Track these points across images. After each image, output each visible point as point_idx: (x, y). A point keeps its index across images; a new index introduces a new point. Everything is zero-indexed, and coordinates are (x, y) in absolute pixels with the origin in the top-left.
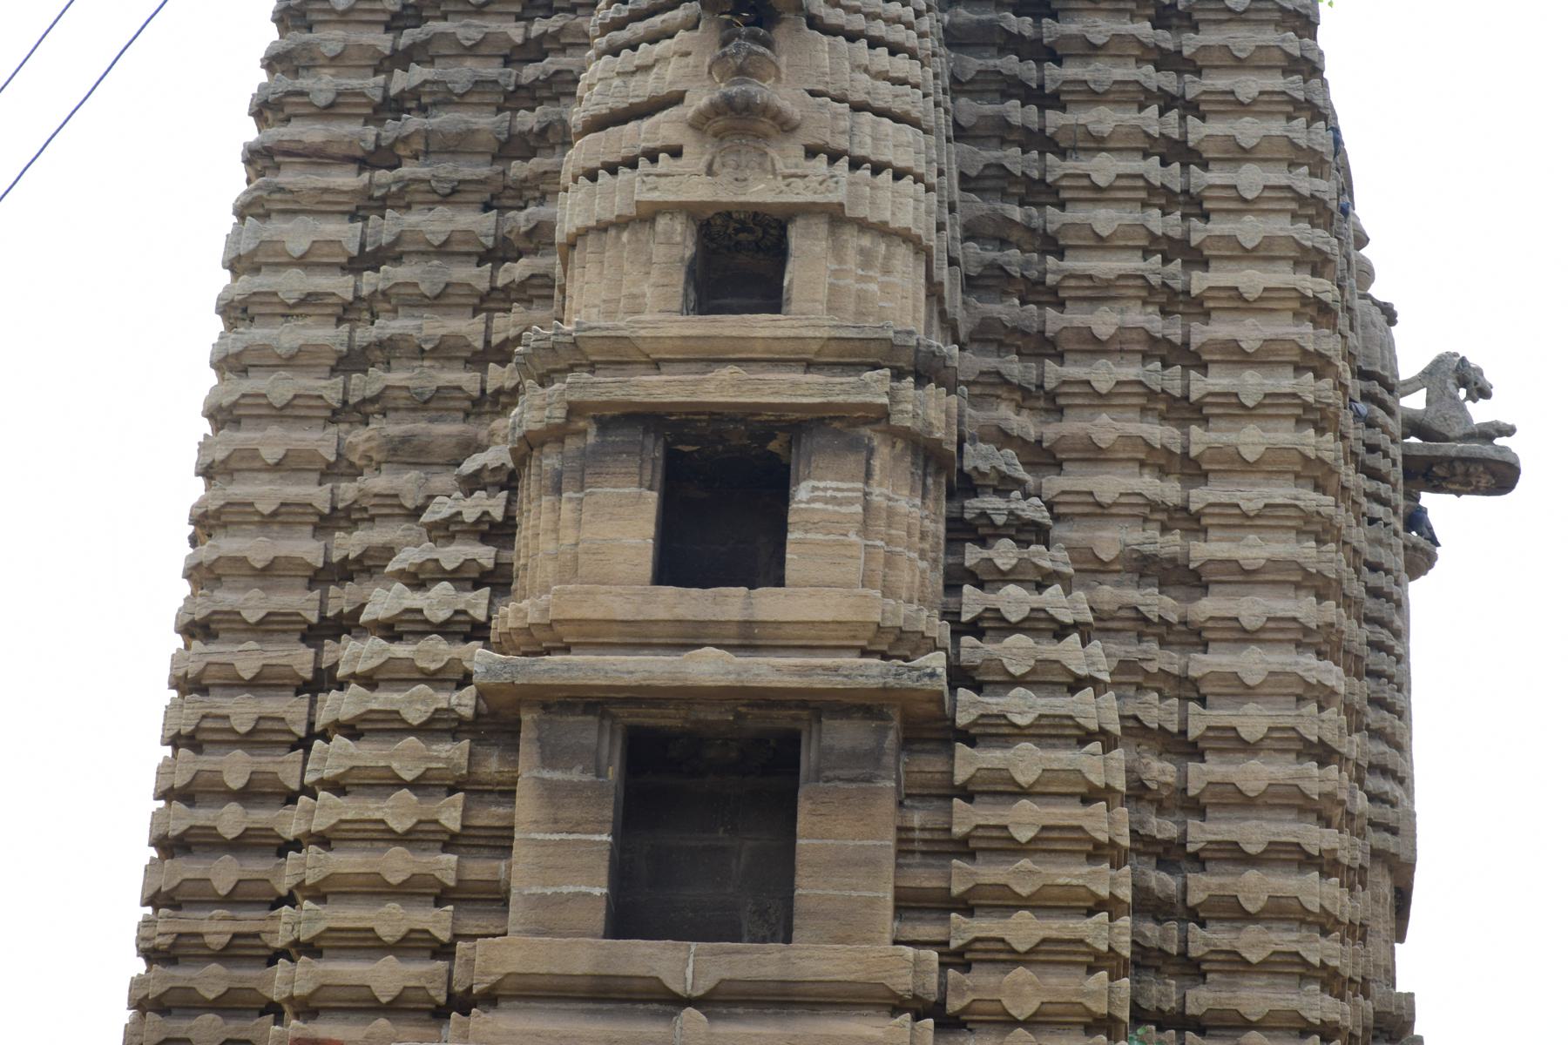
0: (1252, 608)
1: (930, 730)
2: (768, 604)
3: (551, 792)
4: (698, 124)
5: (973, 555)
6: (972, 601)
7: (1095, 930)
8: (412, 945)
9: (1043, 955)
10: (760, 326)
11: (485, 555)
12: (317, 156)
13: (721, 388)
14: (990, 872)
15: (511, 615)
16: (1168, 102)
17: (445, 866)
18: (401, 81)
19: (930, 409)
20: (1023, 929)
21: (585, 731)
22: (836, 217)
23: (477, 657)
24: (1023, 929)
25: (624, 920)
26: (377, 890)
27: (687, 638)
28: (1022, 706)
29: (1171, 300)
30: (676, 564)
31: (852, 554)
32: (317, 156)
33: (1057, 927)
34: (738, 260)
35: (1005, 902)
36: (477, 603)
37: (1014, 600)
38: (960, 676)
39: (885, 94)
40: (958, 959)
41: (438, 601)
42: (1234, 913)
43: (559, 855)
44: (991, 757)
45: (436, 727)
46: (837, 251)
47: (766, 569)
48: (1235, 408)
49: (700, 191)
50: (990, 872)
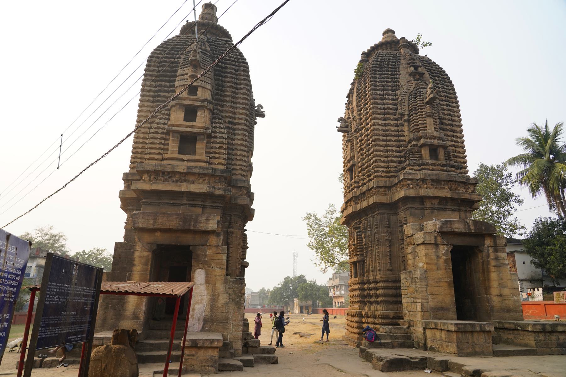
0: (240, 127)
1: (209, 136)
2: (194, 124)
3: (173, 140)
4: (189, 77)
5: (214, 121)
7: (223, 156)
8: (159, 154)
9: (219, 158)
10: (195, 97)
11: (167, 117)
12: (151, 75)
13: (190, 103)
14: (214, 150)
15: (169, 123)
16: (235, 78)
17: (162, 146)
18: (160, 69)
19: (211, 106)
20: (217, 156)
21: (176, 135)
22: (202, 87)
23: (166, 127)
24: (217, 156)
25: (179, 153)
26: (156, 148)
27: (187, 126)
28: (218, 135)
29: (234, 97)
31: (202, 119)
32: (151, 75)
33: (220, 156)
34: (193, 90)
35: (215, 153)
36: (166, 122)
37: (218, 125)
38: (212, 132)
40: (211, 158)
41: (162, 121)
43: (173, 146)
44: (215, 139)
45: (162, 133)
46: (202, 90)
47: (194, 121)
48: (239, 108)
50: (214, 150)
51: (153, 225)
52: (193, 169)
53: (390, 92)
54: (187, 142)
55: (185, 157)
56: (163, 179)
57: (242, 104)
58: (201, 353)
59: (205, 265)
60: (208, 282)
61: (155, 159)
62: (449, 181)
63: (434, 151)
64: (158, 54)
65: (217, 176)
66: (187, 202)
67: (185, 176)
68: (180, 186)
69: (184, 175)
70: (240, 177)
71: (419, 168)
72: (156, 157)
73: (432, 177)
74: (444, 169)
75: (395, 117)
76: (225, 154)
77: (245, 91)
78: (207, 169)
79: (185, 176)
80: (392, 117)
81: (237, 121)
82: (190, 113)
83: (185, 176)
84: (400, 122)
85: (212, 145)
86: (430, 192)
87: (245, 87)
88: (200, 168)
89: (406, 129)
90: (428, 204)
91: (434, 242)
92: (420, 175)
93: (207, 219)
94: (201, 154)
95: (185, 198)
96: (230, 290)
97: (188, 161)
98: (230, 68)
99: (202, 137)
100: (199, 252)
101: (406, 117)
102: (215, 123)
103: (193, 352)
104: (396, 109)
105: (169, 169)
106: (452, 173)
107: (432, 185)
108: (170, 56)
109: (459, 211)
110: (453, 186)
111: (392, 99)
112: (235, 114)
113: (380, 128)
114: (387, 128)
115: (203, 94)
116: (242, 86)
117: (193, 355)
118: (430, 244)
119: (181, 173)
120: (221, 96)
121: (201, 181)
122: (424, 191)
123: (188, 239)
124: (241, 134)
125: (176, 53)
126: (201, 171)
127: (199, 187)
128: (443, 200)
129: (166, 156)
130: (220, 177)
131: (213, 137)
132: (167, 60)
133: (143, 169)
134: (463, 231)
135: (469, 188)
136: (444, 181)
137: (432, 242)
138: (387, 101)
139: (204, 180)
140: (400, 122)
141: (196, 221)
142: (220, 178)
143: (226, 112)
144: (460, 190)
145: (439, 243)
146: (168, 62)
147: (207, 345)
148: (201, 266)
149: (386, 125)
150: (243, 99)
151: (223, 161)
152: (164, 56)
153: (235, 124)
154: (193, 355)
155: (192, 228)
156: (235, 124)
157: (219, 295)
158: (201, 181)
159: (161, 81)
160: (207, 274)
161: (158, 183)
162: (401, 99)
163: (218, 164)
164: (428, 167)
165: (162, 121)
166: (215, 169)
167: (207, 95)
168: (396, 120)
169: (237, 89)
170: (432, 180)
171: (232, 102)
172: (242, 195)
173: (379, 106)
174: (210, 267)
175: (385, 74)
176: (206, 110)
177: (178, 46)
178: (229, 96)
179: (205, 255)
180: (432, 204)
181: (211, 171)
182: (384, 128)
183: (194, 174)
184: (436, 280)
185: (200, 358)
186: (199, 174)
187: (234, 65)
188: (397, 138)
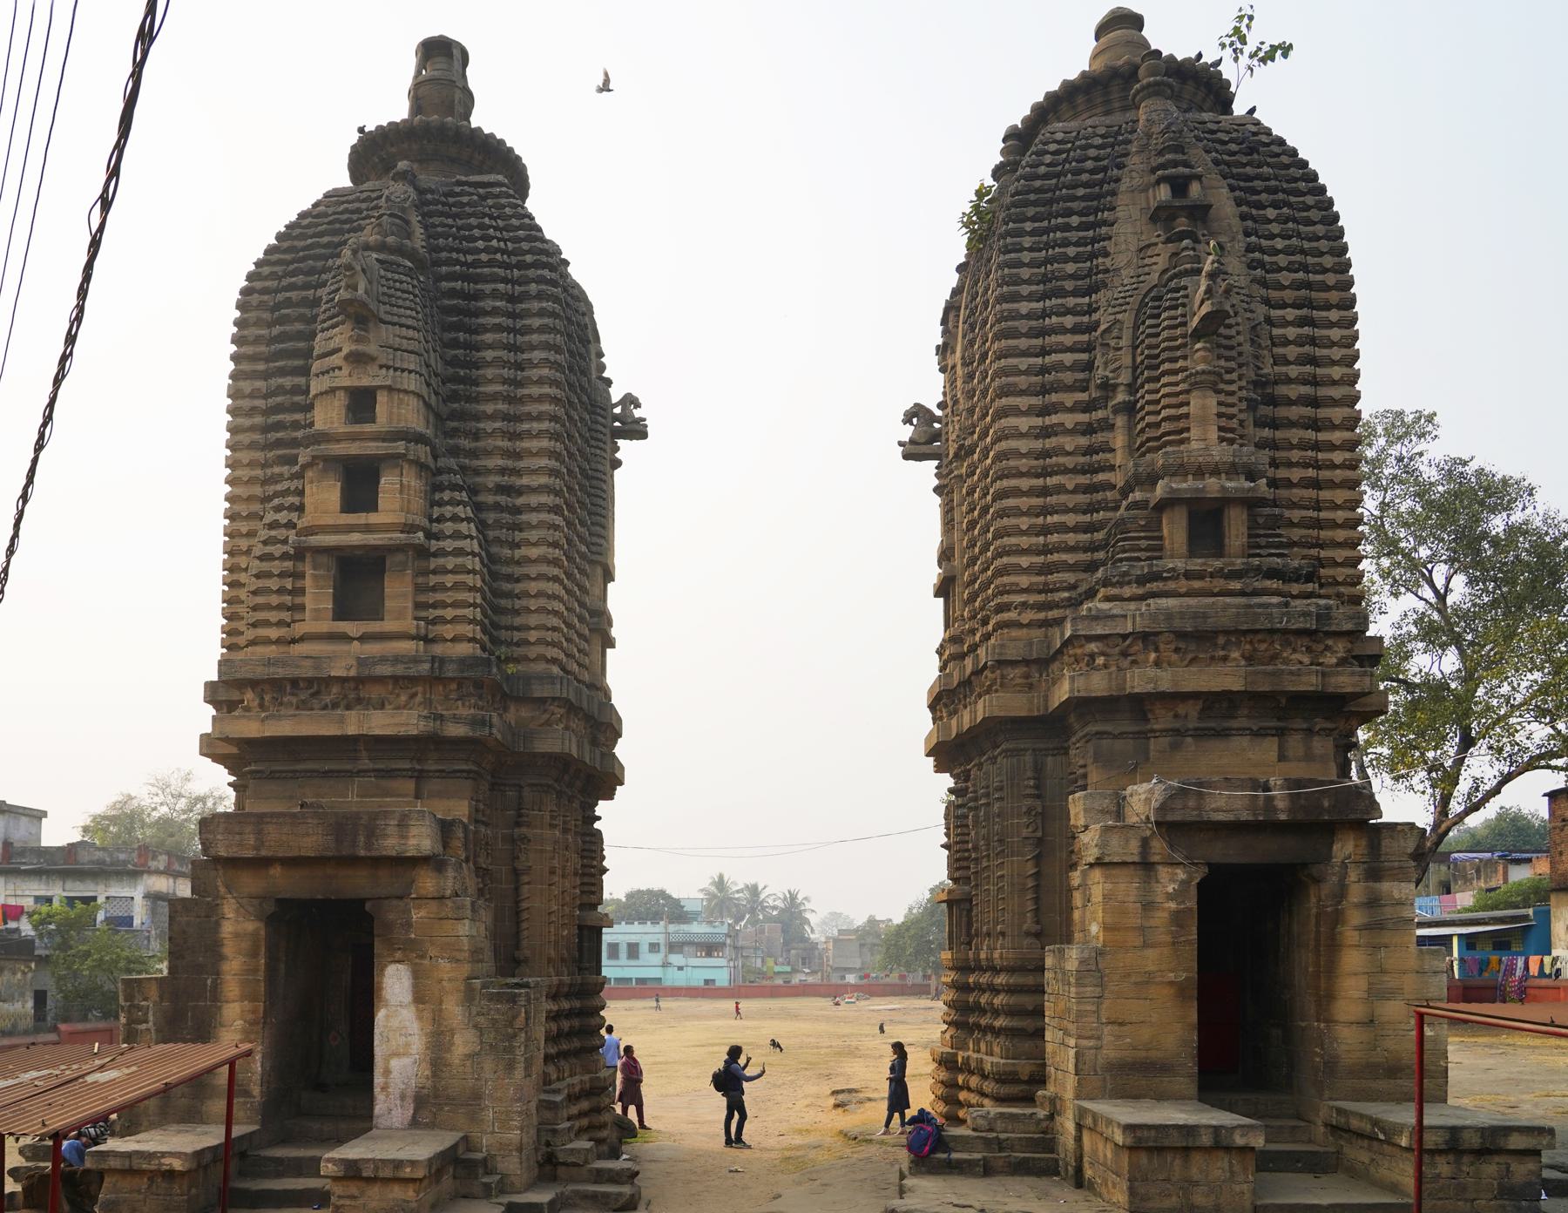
1: (422, 553)
2: (373, 518)
3: (315, 577)
6: (436, 512)
7: (468, 612)
8: (281, 623)
9: (455, 620)
14: (439, 596)
16: (509, 330)
17: (288, 599)
19: (423, 452)
20: (449, 613)
21: (323, 559)
23: (292, 536)
24: (449, 613)
26: (268, 607)
27: (350, 529)
28: (449, 545)
29: (510, 400)
30: (349, 505)
31: (397, 498)
33: (460, 612)
35: (444, 605)
36: (294, 516)
37: (448, 510)
40: (434, 621)
41: (283, 517)
42: (527, 594)
43: (318, 597)
44: (441, 561)
45: (285, 556)
48: (529, 435)
50: (439, 596)
52: (375, 664)
54: (357, 577)
55: (351, 628)
56: (294, 700)
57: (539, 418)
58: (375, 1191)
61: (267, 641)
64: (266, 278)
65: (452, 679)
66: (371, 766)
67: (357, 689)
68: (342, 721)
69: (352, 685)
70: (540, 667)
71: (1140, 591)
72: (273, 633)
75: (1084, 396)
76: (475, 605)
77: (545, 372)
78: (416, 660)
79: (356, 688)
80: (1069, 399)
81: (525, 481)
82: (359, 485)
83: (357, 689)
84: (1100, 414)
85: (433, 580)
86: (1165, 680)
87: (543, 355)
88: (397, 659)
89: (1119, 440)
90: (1162, 719)
93: (403, 824)
94: (400, 615)
95: (364, 754)
97: (363, 638)
98: (495, 295)
99: (400, 557)
101: (1121, 397)
102: (441, 504)
103: (353, 1189)
104: (1089, 366)
108: (300, 279)
109: (1281, 733)
111: (1076, 330)
112: (517, 455)
114: (1051, 443)
115: (401, 412)
116: (537, 355)
117: (353, 1197)
119: (342, 680)
120: (469, 399)
121: (403, 698)
122: (1140, 679)
124: (540, 525)
125: (320, 264)
126: (400, 670)
127: (397, 720)
129: (299, 629)
130: (460, 682)
131: (435, 555)
132: (293, 295)
133: (238, 676)
138: (1054, 339)
139: (413, 696)
140: (1100, 414)
141: (372, 833)
142: (460, 686)
143: (488, 453)
146: (298, 305)
149: (1046, 432)
150: (540, 399)
151: (467, 630)
152: (285, 282)
153: (519, 492)
154: (353, 1197)
155: (362, 853)
156: (519, 492)
158: (403, 698)
159: (282, 372)
161: (279, 718)
163: (453, 640)
165: (283, 517)
166: (442, 661)
167: (411, 416)
168: (1088, 407)
169: (519, 366)
171: (506, 417)
172: (548, 723)
173: (1023, 363)
176: (406, 466)
177: (325, 239)
180: (1176, 716)
181: (427, 666)
183: (380, 680)
185: (374, 1204)
186: (395, 679)
187: (505, 281)
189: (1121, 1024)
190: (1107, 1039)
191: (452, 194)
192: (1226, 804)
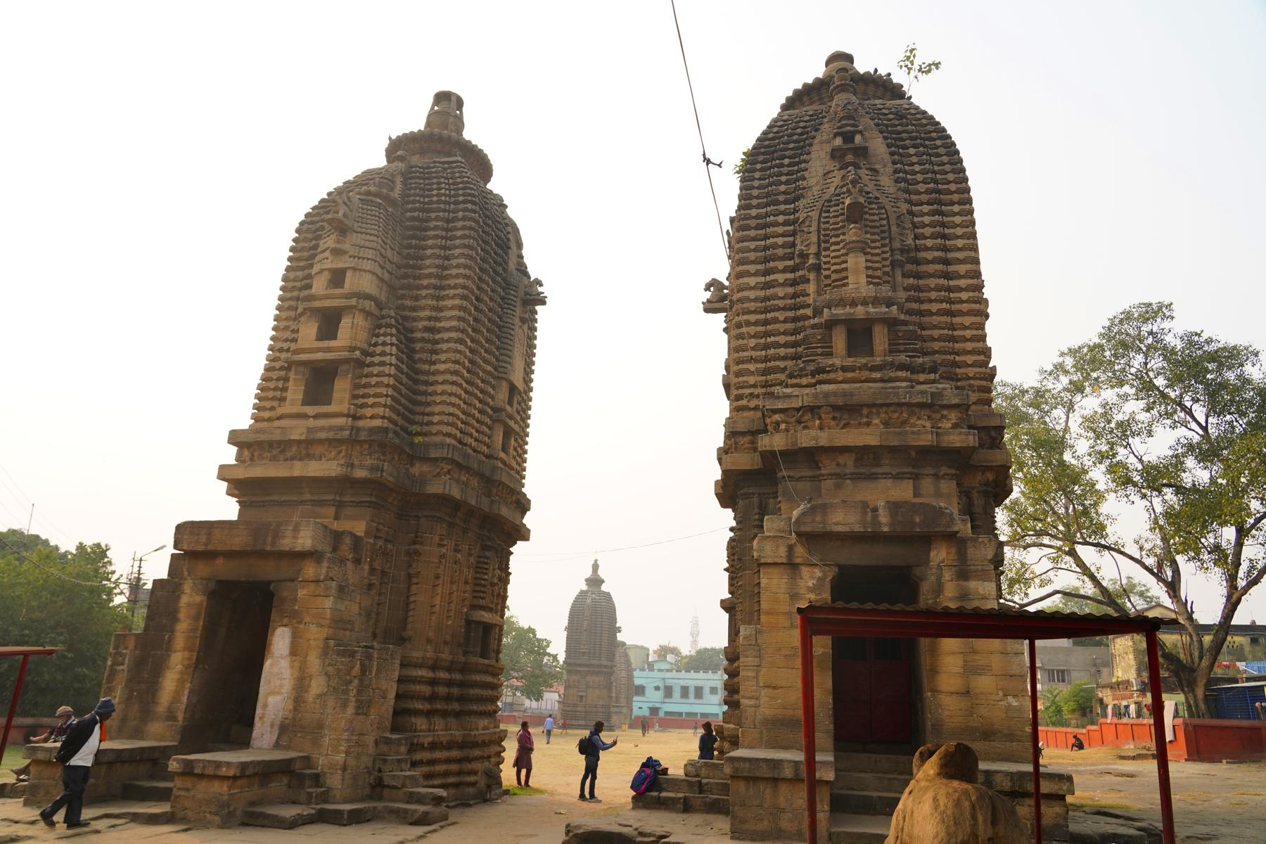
0: (446, 335)
1: (361, 364)
2: (333, 343)
3: (295, 380)
13: (327, 303)
14: (366, 391)
15: (293, 346)
19: (368, 305)
20: (371, 401)
21: (301, 369)
22: (354, 269)
25: (306, 402)
30: (320, 337)
31: (350, 332)
34: (337, 278)
39: (367, 244)
42: (435, 393)
49: (329, 266)
50: (366, 391)
51: (206, 545)
53: (782, 207)
54: (320, 379)
55: (310, 410)
57: (455, 287)
58: (202, 785)
59: (294, 619)
60: (294, 652)
62: (882, 405)
63: (859, 335)
65: (365, 441)
70: (438, 439)
71: (813, 381)
73: (832, 400)
74: (877, 375)
75: (791, 263)
77: (462, 261)
78: (342, 429)
80: (780, 265)
81: (442, 324)
84: (801, 273)
85: (364, 380)
86: (823, 438)
87: (461, 251)
88: (330, 428)
89: (811, 288)
90: (828, 466)
91: (784, 561)
92: (801, 396)
93: (296, 530)
96: (330, 669)
97: (316, 417)
98: (437, 219)
99: (346, 367)
100: (285, 594)
101: (812, 261)
102: (378, 336)
103: (188, 783)
104: (793, 245)
105: (277, 436)
106: (897, 384)
107: (834, 418)
109: (916, 477)
110: (895, 415)
111: (785, 223)
112: (440, 309)
113: (752, 294)
114: (769, 292)
116: (457, 252)
117: (187, 790)
118: (775, 564)
119: (299, 442)
120: (415, 278)
122: (806, 438)
123: (266, 570)
126: (331, 435)
128: (863, 453)
130: (370, 443)
131: (369, 366)
134: (858, 528)
135: (943, 417)
136: (869, 406)
137: (779, 561)
138: (772, 229)
139: (339, 452)
140: (801, 273)
141: (277, 535)
142: (370, 446)
143: (423, 309)
144: (913, 425)
145: (798, 561)
147: (210, 771)
148: (285, 621)
149: (767, 286)
150: (457, 276)
153: (439, 331)
154: (187, 790)
155: (268, 548)
156: (439, 331)
157: (311, 677)
160: (295, 636)
162: (853, 218)
163: (371, 418)
164: (832, 376)
166: (359, 430)
168: (793, 269)
169: (447, 258)
170: (836, 408)
171: (435, 287)
172: (438, 475)
173: (753, 245)
174: (300, 623)
175: (777, 166)
178: (429, 276)
179: (295, 600)
180: (838, 465)
181: (347, 433)
182: (761, 293)
183: (321, 441)
184: (784, 652)
185: (200, 796)
187: (444, 211)
188: (790, 314)
189: (775, 688)
190: (764, 700)
191: (428, 168)
192: (842, 520)
